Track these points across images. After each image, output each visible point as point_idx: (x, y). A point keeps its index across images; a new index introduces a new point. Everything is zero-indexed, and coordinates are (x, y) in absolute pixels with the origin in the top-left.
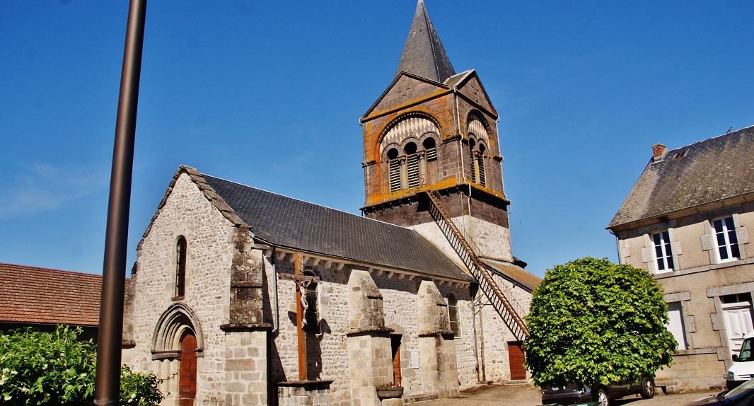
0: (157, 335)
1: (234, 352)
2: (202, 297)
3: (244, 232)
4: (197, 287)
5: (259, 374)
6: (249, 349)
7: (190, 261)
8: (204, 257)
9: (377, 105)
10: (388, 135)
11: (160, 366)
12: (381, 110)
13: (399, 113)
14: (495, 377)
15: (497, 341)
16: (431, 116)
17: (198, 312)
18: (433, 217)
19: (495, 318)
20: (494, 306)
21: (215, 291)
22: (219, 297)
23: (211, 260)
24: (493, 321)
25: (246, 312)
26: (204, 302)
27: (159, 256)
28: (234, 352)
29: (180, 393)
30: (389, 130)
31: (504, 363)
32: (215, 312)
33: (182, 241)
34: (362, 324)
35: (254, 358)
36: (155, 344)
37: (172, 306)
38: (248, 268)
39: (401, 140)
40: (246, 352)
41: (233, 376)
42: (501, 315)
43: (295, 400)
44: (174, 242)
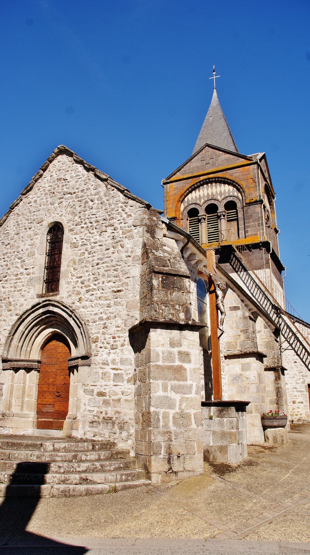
0: (12, 339)
1: (161, 355)
2: (87, 291)
3: (155, 216)
4: (80, 280)
5: (191, 386)
6: (180, 353)
7: (70, 249)
8: (93, 245)
9: (179, 170)
10: (190, 196)
11: (13, 378)
12: (183, 174)
13: (202, 178)
14: (295, 417)
15: (297, 383)
16: (234, 182)
17: (82, 310)
18: (235, 269)
19: (295, 362)
20: (295, 351)
21: (111, 284)
22: (119, 291)
23: (104, 248)
24: (293, 365)
25: (173, 306)
26: (93, 298)
27: (18, 247)
28: (161, 355)
29: (37, 413)
30: (191, 192)
31: (304, 404)
32: (111, 310)
33: (56, 231)
34: (242, 345)
35: (186, 365)
36: (8, 351)
37: (39, 304)
38: (166, 254)
39: (203, 201)
40: (177, 356)
41: (161, 388)
42: (302, 360)
43: (221, 424)
44: (44, 229)
